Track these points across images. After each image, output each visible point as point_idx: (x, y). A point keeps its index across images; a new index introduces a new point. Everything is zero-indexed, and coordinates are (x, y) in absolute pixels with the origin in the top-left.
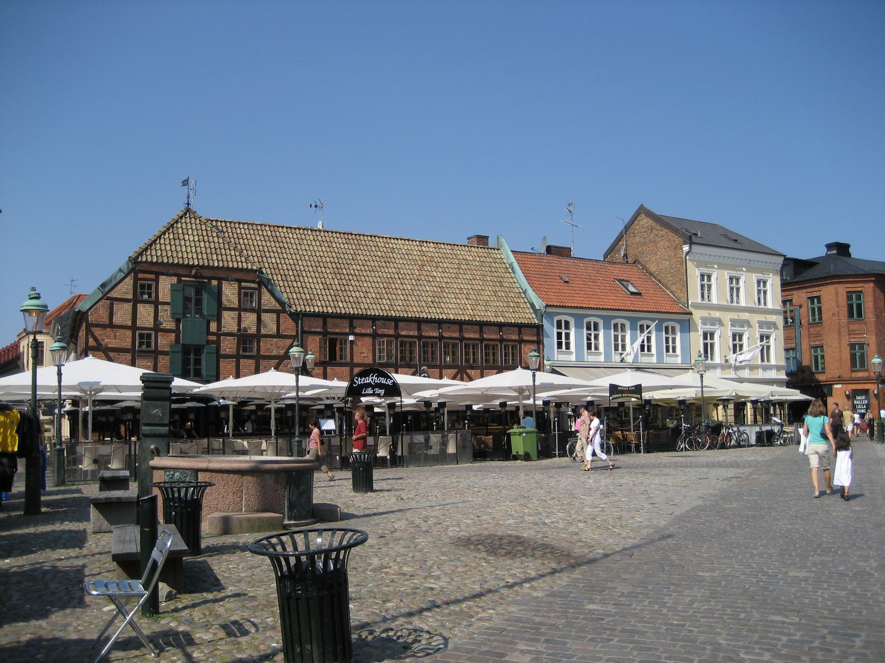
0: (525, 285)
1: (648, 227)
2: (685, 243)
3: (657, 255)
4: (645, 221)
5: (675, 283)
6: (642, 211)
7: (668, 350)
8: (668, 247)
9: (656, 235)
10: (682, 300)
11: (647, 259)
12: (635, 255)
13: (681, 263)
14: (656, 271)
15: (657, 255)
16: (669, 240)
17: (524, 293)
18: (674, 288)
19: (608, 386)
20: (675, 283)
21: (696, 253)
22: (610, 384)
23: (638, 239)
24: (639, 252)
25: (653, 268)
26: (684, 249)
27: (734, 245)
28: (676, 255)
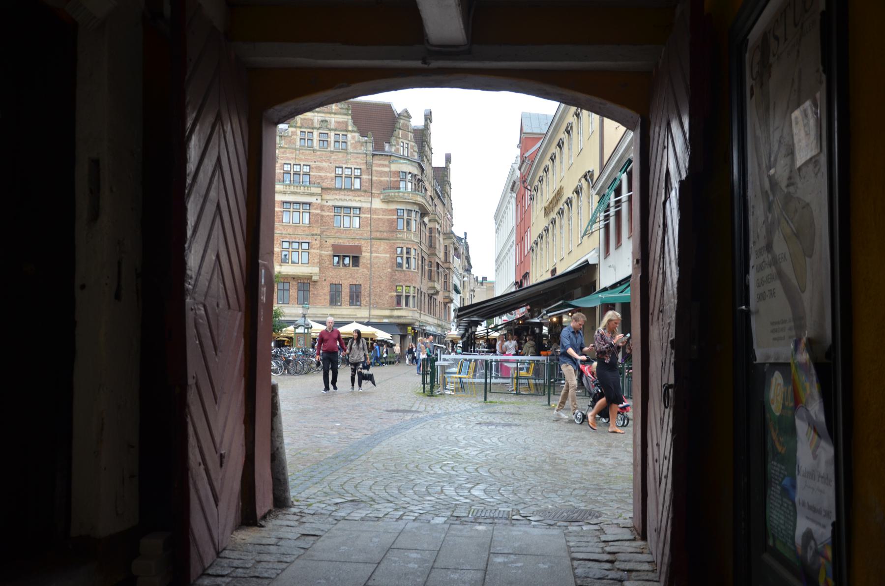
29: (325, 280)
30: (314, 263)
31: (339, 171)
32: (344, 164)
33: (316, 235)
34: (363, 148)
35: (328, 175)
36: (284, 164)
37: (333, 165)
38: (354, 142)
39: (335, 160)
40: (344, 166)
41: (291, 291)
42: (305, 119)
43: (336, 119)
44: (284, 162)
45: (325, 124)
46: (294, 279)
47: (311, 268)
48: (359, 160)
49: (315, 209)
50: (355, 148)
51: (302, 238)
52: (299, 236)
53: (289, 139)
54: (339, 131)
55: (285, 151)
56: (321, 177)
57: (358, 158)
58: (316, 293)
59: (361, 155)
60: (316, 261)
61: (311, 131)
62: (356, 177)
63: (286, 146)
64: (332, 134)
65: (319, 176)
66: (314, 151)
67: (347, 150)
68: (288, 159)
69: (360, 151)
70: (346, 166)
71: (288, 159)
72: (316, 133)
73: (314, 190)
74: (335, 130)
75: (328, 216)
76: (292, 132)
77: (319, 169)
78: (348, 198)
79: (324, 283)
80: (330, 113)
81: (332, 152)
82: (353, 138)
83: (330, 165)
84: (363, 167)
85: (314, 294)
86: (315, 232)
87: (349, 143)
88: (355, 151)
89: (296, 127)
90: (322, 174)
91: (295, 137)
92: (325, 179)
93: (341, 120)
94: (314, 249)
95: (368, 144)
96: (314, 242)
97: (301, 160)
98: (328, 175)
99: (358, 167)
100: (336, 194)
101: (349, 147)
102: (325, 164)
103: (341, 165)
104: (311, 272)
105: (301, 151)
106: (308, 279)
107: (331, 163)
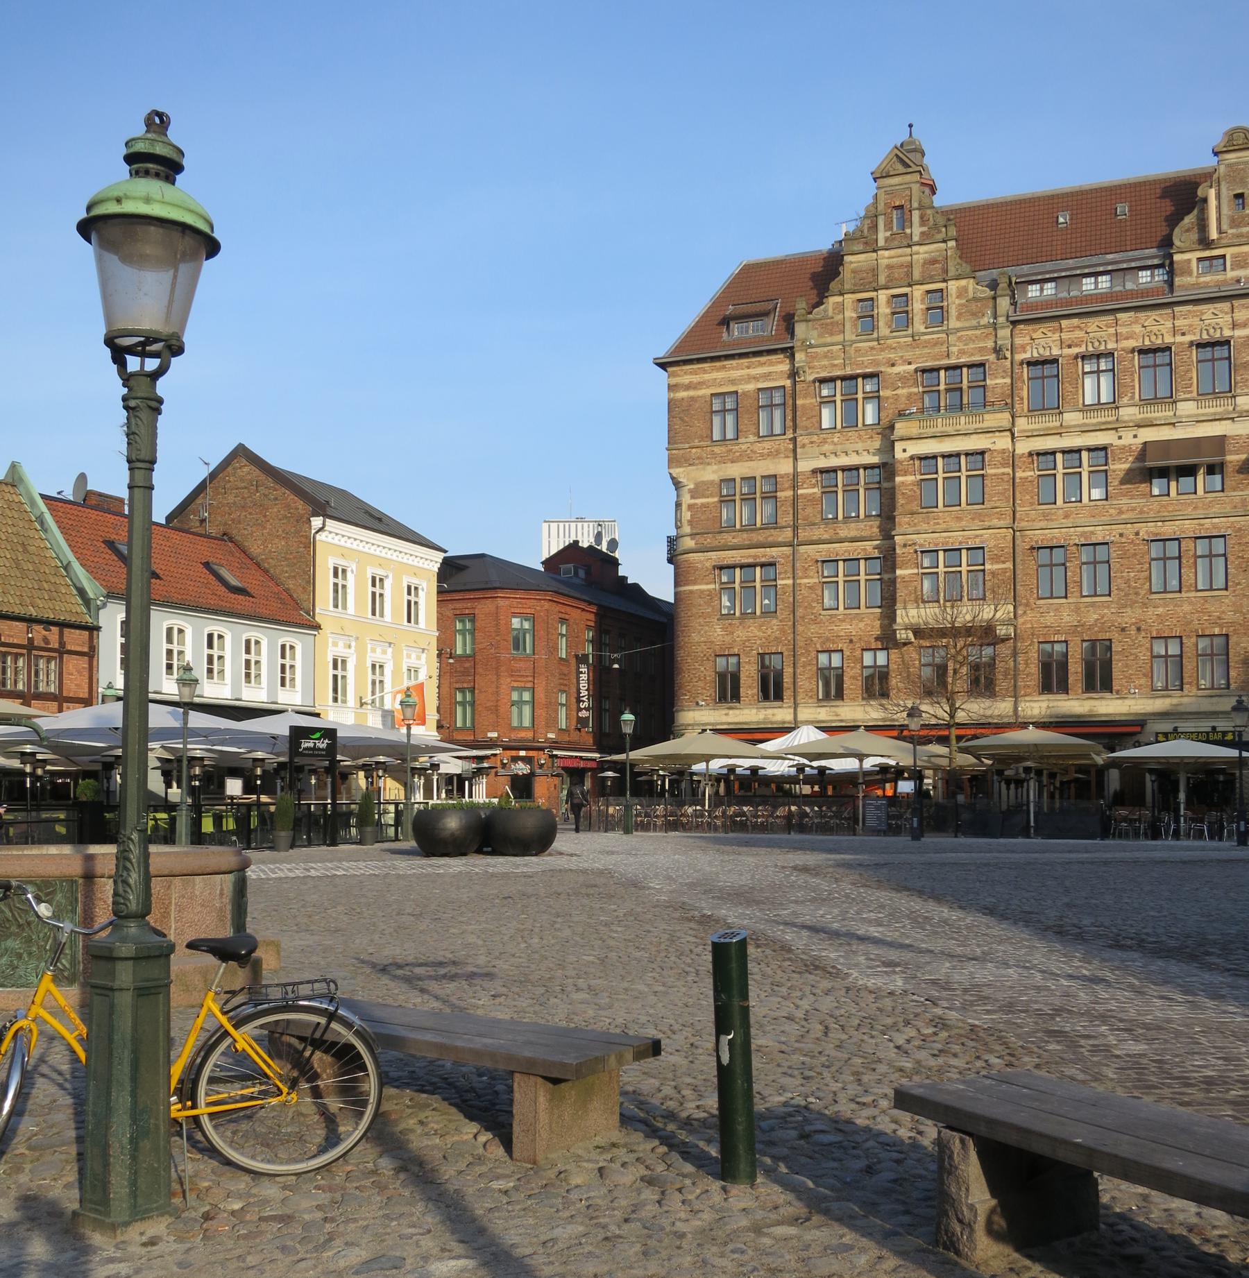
0: (71, 557)
1: (251, 481)
2: (316, 514)
3: (265, 528)
4: (246, 469)
5: (294, 577)
6: (241, 453)
7: (283, 684)
8: (285, 517)
9: (265, 495)
10: (305, 605)
11: (246, 532)
12: (226, 524)
13: (307, 546)
14: (261, 554)
15: (265, 528)
16: (288, 506)
17: (66, 568)
18: (291, 584)
19: (287, 733)
20: (294, 577)
21: (330, 532)
22: (291, 727)
23: (231, 499)
24: (233, 520)
25: (255, 549)
26: (313, 523)
27: (377, 525)
28: (297, 532)
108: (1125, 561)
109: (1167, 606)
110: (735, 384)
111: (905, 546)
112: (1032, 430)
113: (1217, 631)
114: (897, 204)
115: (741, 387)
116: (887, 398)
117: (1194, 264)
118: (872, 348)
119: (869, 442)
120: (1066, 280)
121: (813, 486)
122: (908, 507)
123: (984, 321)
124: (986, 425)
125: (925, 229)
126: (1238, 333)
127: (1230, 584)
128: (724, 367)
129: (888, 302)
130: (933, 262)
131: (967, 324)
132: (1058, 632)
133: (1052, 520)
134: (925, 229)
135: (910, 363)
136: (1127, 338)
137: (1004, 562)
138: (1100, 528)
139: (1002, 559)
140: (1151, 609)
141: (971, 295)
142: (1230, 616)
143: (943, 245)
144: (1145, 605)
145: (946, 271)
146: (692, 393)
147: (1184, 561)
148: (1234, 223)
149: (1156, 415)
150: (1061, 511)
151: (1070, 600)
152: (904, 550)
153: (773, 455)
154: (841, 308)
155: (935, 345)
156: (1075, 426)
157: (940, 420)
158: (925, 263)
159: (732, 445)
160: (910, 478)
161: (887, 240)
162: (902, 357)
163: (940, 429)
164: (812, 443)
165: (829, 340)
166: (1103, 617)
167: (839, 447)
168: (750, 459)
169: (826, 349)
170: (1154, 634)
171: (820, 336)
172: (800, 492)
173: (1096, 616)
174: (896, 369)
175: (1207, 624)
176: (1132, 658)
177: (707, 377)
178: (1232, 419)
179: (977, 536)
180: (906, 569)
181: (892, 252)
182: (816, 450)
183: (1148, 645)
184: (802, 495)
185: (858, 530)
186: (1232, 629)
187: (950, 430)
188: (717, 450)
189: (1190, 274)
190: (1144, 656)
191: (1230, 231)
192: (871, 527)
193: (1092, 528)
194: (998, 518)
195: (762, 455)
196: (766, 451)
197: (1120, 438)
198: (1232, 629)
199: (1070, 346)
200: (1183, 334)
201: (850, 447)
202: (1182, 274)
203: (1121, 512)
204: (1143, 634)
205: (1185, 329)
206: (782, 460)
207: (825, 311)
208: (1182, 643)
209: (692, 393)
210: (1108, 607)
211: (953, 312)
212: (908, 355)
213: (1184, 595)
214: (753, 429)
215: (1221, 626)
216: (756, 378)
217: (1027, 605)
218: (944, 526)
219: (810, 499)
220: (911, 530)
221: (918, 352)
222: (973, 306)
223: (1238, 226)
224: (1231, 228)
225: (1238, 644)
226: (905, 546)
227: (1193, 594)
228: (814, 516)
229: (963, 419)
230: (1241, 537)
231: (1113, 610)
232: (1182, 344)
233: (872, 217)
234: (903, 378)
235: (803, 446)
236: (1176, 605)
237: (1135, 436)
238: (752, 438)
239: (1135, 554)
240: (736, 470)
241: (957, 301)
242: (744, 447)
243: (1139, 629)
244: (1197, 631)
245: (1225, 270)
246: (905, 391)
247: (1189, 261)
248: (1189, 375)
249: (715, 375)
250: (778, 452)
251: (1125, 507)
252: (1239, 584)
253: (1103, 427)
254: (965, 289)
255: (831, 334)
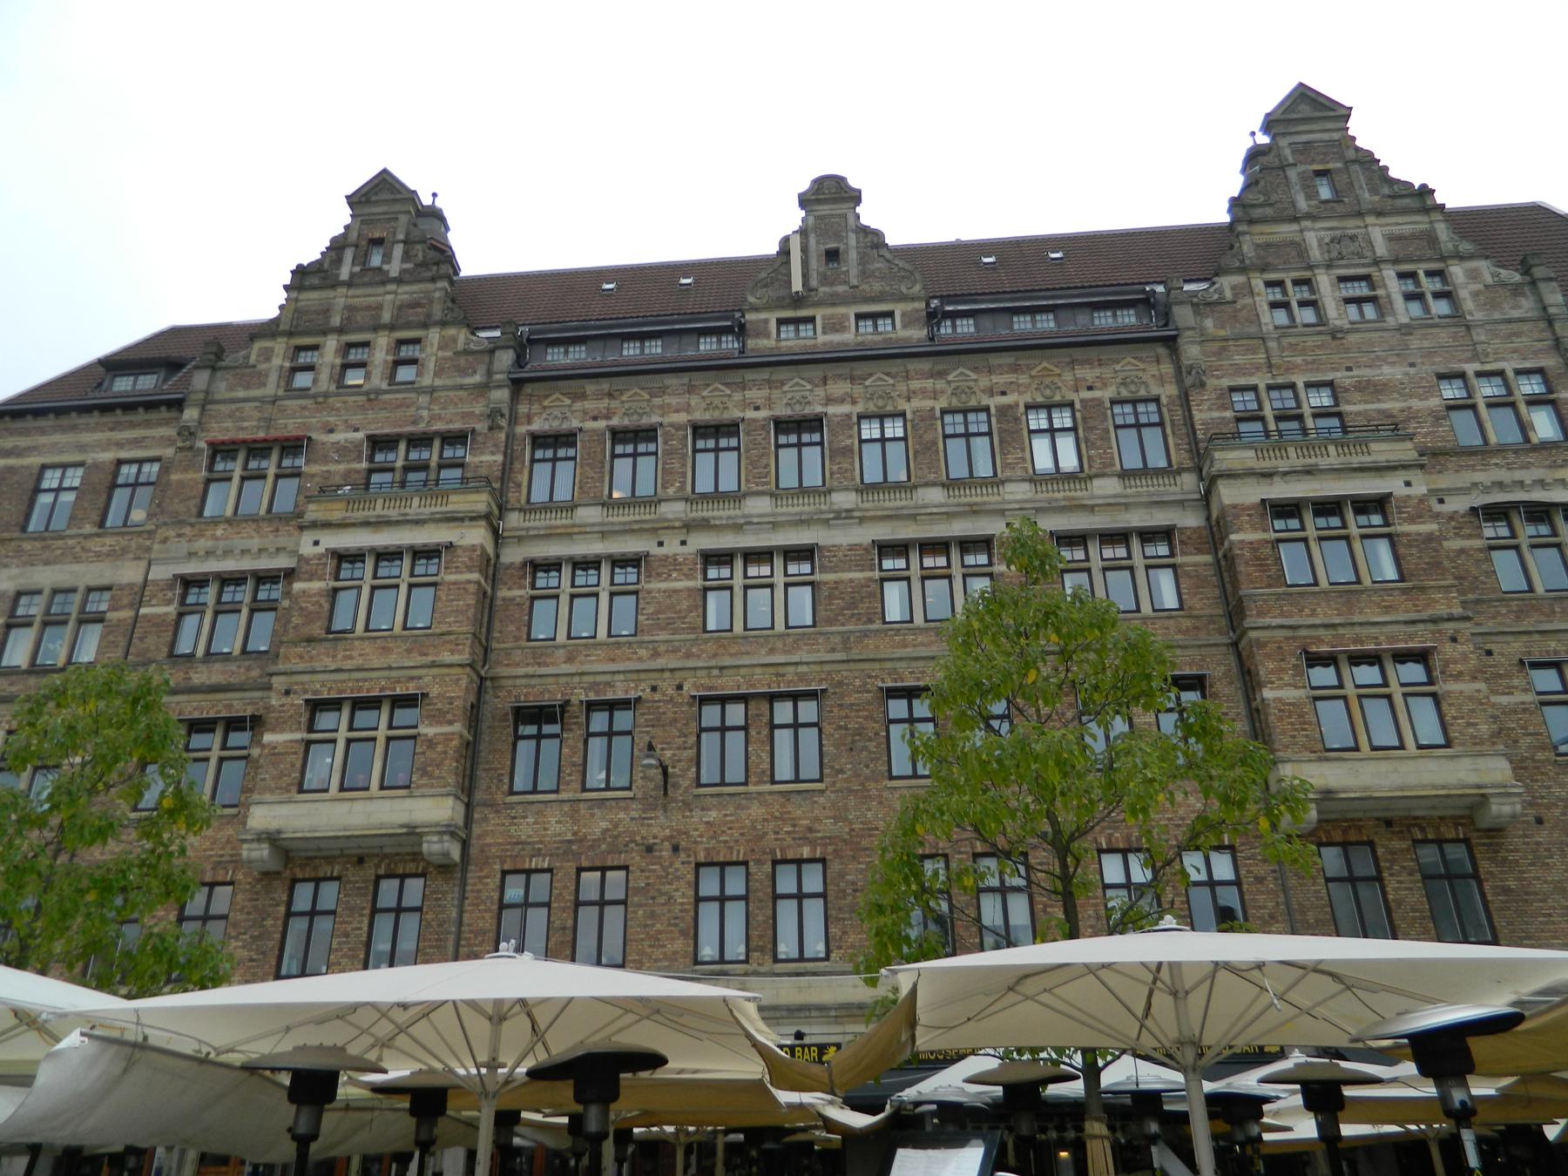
29: (1539, 821)
30: (1477, 741)
31: (1451, 391)
32: (1469, 361)
33: (1451, 619)
34: (1523, 301)
35: (1416, 404)
36: (1232, 389)
37: (1426, 370)
38: (1480, 286)
39: (1429, 354)
40: (1471, 368)
41: (1391, 884)
42: (1268, 245)
43: (1387, 230)
44: (1226, 382)
45: (1353, 247)
46: (1389, 823)
47: (1466, 763)
48: (1521, 342)
49: (1412, 520)
50: (1493, 305)
51: (1392, 638)
52: (1374, 630)
53: (1228, 308)
54: (1412, 261)
55: (1224, 349)
56: (1386, 414)
57: (1518, 334)
58: (1512, 884)
59: (1525, 327)
60: (1484, 727)
61: (1307, 274)
62: (1533, 401)
63: (1222, 333)
64: (1389, 274)
65: (1379, 411)
66: (1335, 334)
67: (1462, 316)
68: (1239, 370)
69: (1516, 314)
70: (1477, 366)
71: (1239, 370)
72: (1324, 281)
73: (1382, 451)
74: (1396, 262)
75: (1462, 551)
76: (1233, 288)
77: (1374, 389)
78: (1527, 476)
79: (1542, 836)
80: (1360, 214)
81: (1406, 330)
82: (1473, 275)
83: (1412, 371)
84: (1550, 362)
85: (1507, 891)
86: (1441, 610)
87: (1464, 294)
88: (1497, 316)
89: (1243, 270)
90: (1392, 405)
91: (1248, 300)
92: (1409, 419)
93: (1407, 229)
94: (1458, 677)
95: (1541, 285)
96: (1448, 649)
97: (1290, 368)
98: (1416, 404)
99: (1528, 365)
100: (1473, 468)
101: (1469, 305)
102: (1391, 372)
103: (1456, 366)
104: (1473, 779)
105: (1285, 341)
106: (1456, 821)
107: (1412, 365)
108: (658, 731)
109: (724, 807)
110: (85, 451)
111: (287, 693)
112: (528, 529)
113: (806, 852)
114: (377, 235)
115: (95, 456)
116: (313, 476)
117: (773, 325)
118: (304, 408)
119: (271, 537)
120: (599, 344)
121: (169, 602)
122: (305, 631)
123: (477, 378)
124: (450, 508)
125: (409, 266)
126: (831, 410)
127: (826, 771)
128: (73, 428)
129: (337, 351)
130: (414, 305)
131: (449, 382)
132: (538, 853)
133: (546, 665)
134: (409, 266)
135: (356, 430)
136: (677, 411)
137: (450, 723)
138: (621, 677)
139: (449, 717)
140: (697, 813)
141: (460, 346)
142: (827, 827)
143: (430, 286)
144: (687, 806)
145: (429, 316)
146: (12, 462)
147: (753, 733)
148: (825, 280)
149: (716, 513)
150: (561, 651)
151: (563, 796)
152: (284, 700)
153: (116, 555)
154: (267, 355)
155: (398, 407)
156: (593, 525)
157: (380, 502)
158: (400, 308)
159: (53, 539)
160: (317, 585)
161: (352, 275)
162: (346, 421)
163: (379, 511)
164: (179, 536)
165: (241, 394)
166: (616, 826)
167: (221, 543)
168: (77, 560)
169: (233, 406)
170: (702, 858)
171: (231, 388)
172: (143, 611)
173: (604, 825)
174: (339, 437)
175: (789, 840)
176: (662, 900)
177: (43, 440)
178: (827, 521)
179: (412, 678)
180: (282, 731)
181: (358, 291)
182: (183, 547)
183: (691, 877)
184: (145, 616)
185: (224, 672)
186: (830, 849)
187: (393, 513)
188: (27, 546)
189: (768, 336)
190: (683, 896)
191: (822, 289)
192: (249, 669)
193: (607, 678)
194: (452, 652)
195: (98, 555)
196: (105, 549)
197: (661, 544)
198: (830, 849)
199: (595, 418)
200: (757, 408)
201: (239, 543)
202: (757, 335)
203: (656, 655)
204: (683, 856)
205: (759, 402)
206: (127, 564)
207: (247, 357)
208: (748, 874)
209: (12, 462)
210: (626, 809)
211: (431, 365)
212: (356, 419)
213: (751, 788)
214: (95, 517)
215: (813, 844)
216: (120, 445)
217: (491, 805)
218: (358, 662)
219: (156, 622)
220: (301, 666)
221: (371, 415)
222: (462, 361)
223: (832, 284)
224: (823, 285)
225: (842, 875)
226: (287, 693)
227: (768, 787)
228: (158, 649)
229: (416, 501)
230: (842, 696)
231: (634, 814)
232: (754, 420)
233: (337, 246)
234: (343, 451)
235: (165, 541)
236: (739, 807)
237: (683, 543)
238: (88, 529)
239: (675, 721)
240: (46, 577)
241: (440, 354)
242: (70, 542)
243: (676, 849)
244: (773, 852)
245: (815, 333)
246: (342, 467)
247: (766, 321)
248: (764, 461)
249: (58, 438)
250: (124, 551)
251: (662, 648)
252: (841, 771)
253: (635, 527)
254: (454, 340)
255: (247, 387)
